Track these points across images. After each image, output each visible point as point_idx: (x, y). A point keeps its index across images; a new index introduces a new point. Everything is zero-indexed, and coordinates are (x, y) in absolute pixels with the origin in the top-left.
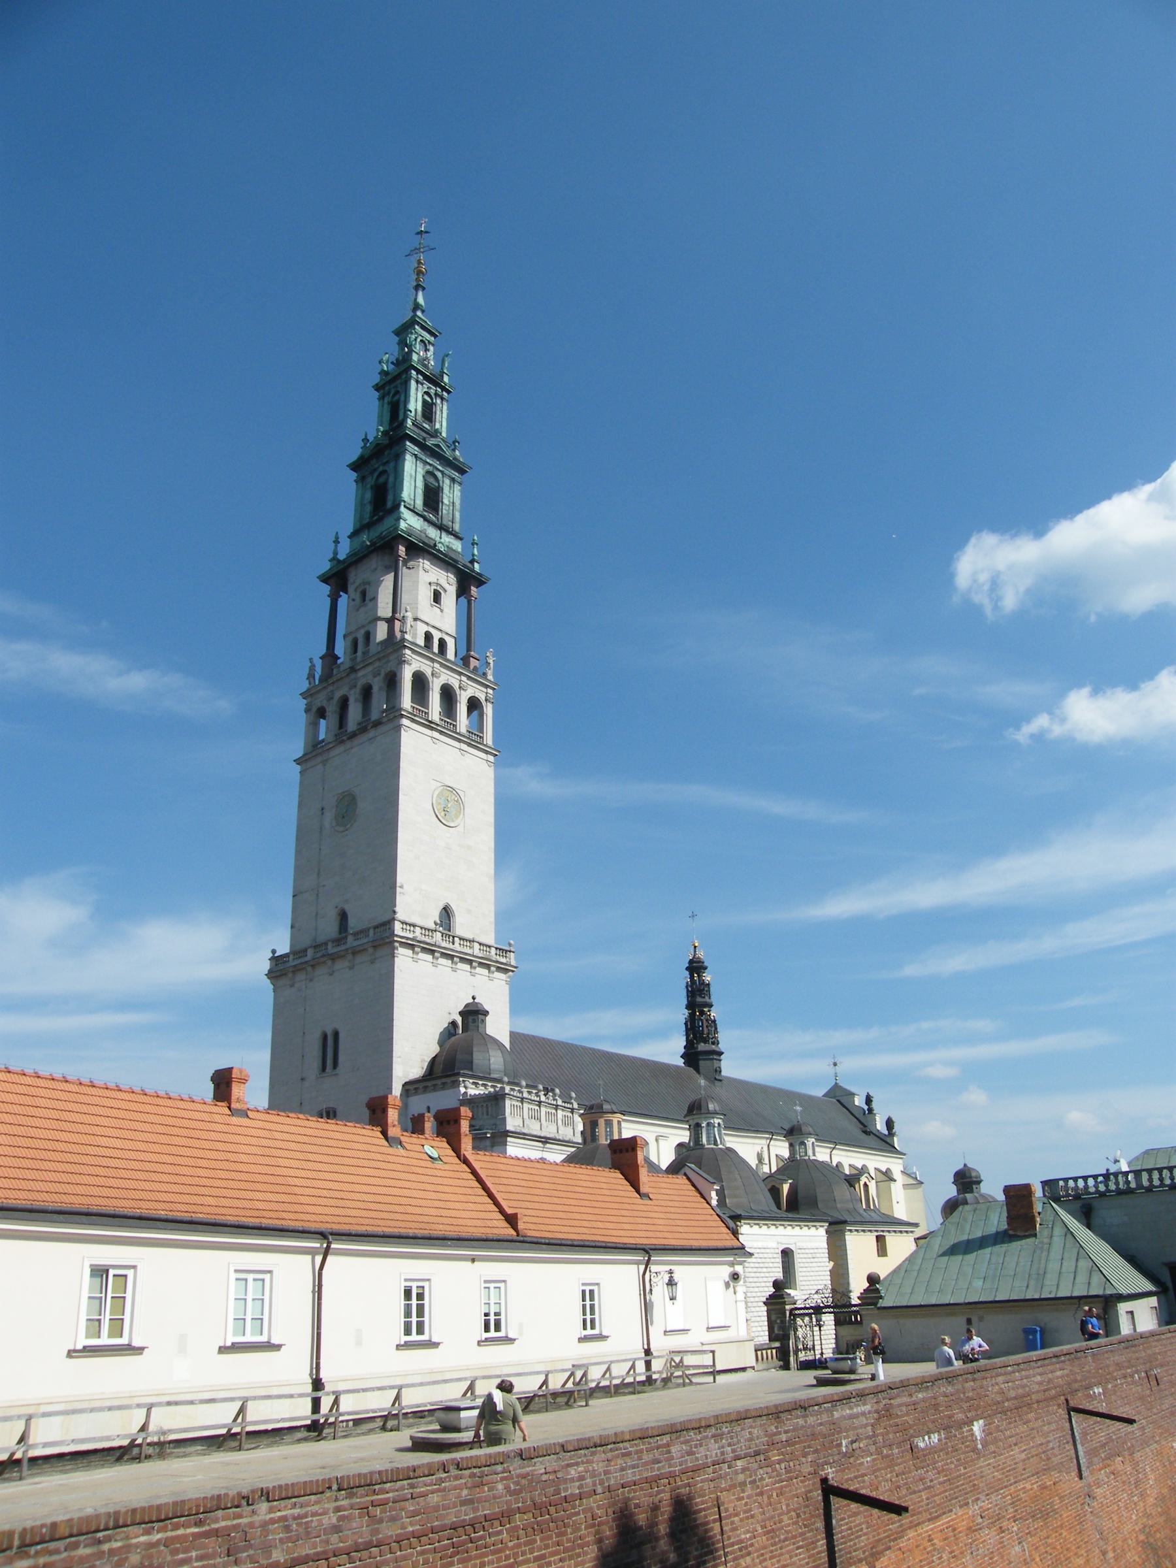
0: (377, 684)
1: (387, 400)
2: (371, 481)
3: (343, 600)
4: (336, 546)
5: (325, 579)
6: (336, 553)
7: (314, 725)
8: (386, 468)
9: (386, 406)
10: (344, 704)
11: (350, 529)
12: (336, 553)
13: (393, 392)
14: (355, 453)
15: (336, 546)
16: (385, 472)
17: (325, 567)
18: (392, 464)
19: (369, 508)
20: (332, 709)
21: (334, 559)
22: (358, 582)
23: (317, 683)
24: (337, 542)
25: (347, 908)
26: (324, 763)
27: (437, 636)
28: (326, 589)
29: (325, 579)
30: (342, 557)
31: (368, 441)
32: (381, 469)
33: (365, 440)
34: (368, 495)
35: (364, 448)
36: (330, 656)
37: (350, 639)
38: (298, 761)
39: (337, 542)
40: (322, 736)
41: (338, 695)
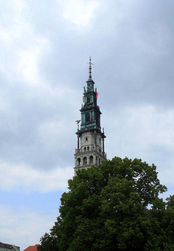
6: (78, 128)
12: (78, 128)
13: (88, 96)
14: (80, 108)
17: (77, 131)
22: (85, 136)
28: (77, 136)
33: (82, 105)
34: (84, 118)
36: (78, 149)
37: (84, 147)
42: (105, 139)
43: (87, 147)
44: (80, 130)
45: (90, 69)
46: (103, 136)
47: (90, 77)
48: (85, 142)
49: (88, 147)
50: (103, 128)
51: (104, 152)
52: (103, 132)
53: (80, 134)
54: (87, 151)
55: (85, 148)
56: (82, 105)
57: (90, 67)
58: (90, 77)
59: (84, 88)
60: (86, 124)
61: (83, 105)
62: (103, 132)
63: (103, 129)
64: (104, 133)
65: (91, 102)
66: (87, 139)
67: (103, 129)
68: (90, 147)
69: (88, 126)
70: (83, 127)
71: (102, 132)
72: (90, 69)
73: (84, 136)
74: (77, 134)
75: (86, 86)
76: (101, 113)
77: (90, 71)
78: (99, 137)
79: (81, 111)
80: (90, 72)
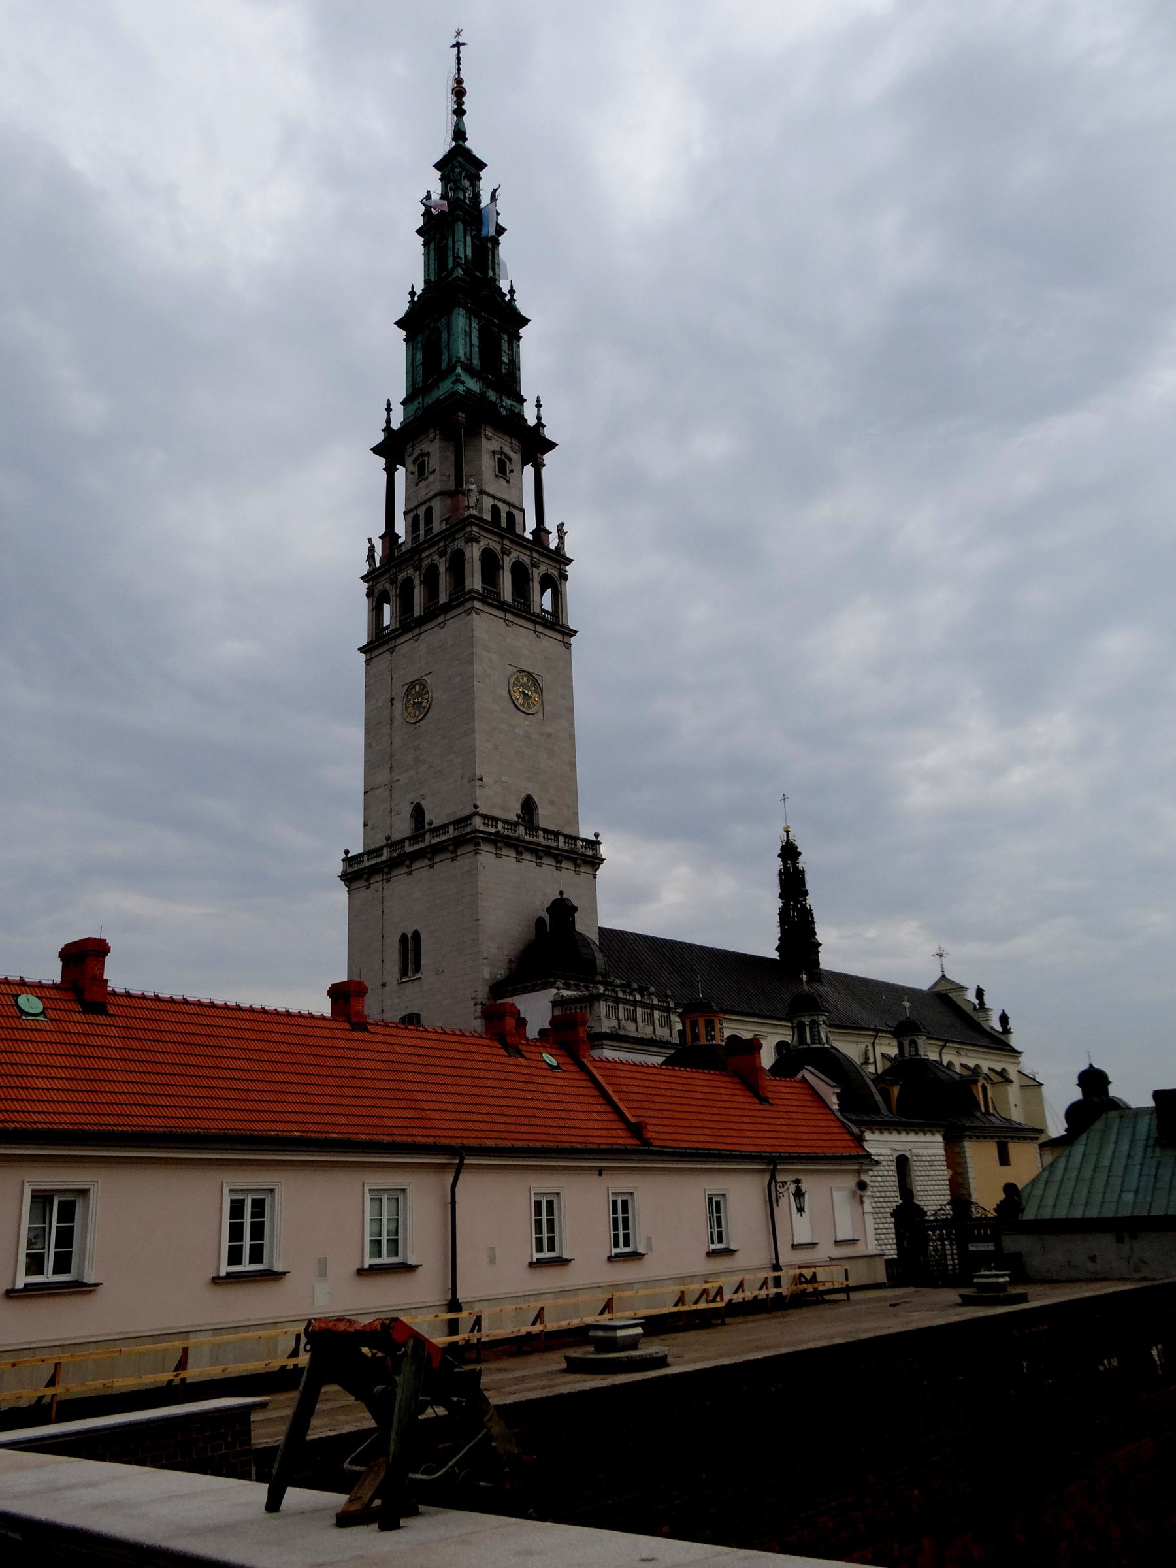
3: (400, 474)
4: (389, 414)
5: (377, 450)
6: (388, 421)
7: (376, 612)
9: (432, 253)
10: (408, 585)
11: (403, 395)
12: (388, 421)
15: (389, 414)
17: (379, 437)
19: (420, 371)
20: (393, 593)
21: (388, 429)
22: (417, 452)
23: (378, 565)
24: (389, 409)
25: (423, 803)
26: (391, 651)
27: (504, 509)
28: (381, 462)
29: (377, 450)
30: (396, 425)
31: (415, 294)
33: (412, 293)
34: (419, 356)
36: (389, 536)
37: (411, 515)
38: (362, 650)
39: (389, 409)
40: (387, 621)
43: (421, 511)
47: (459, 134)
50: (538, 401)
51: (541, 531)
52: (539, 418)
58: (459, 134)
62: (539, 418)
63: (539, 406)
64: (540, 425)
67: (539, 406)
68: (437, 505)
71: (532, 422)
75: (436, 189)
76: (525, 321)
80: (459, 112)
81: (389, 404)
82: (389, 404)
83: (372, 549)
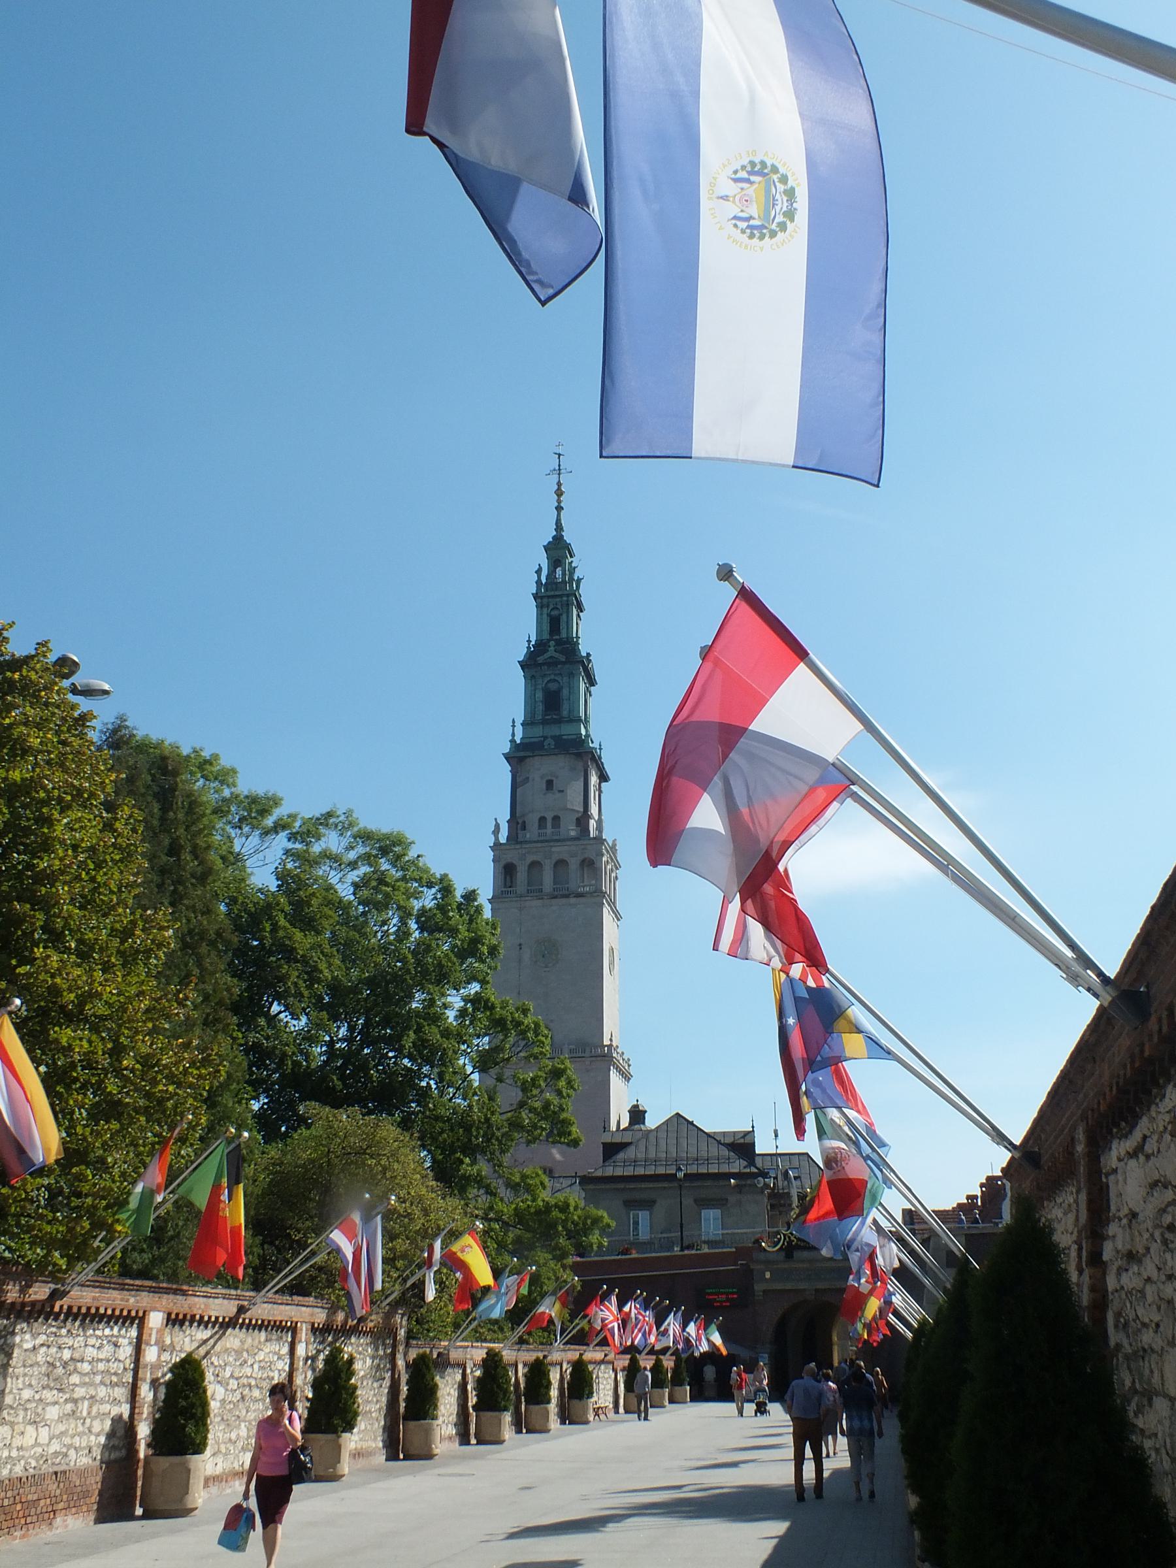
0: (574, 864)
1: (545, 611)
2: (541, 683)
6: (513, 735)
8: (559, 678)
9: (545, 616)
11: (520, 719)
12: (513, 735)
13: (551, 606)
14: (521, 654)
16: (555, 681)
17: (507, 748)
18: (565, 679)
19: (540, 707)
21: (513, 741)
24: (514, 726)
30: (518, 742)
32: (552, 677)
33: (529, 641)
34: (539, 695)
35: (529, 648)
39: (514, 726)
41: (530, 858)
42: (603, 784)
43: (549, 816)
44: (518, 742)
45: (559, 493)
46: (603, 777)
47: (559, 527)
48: (545, 794)
49: (556, 819)
53: (519, 756)
54: (549, 830)
55: (542, 820)
56: (529, 641)
57: (559, 484)
58: (559, 527)
59: (539, 572)
60: (544, 722)
61: (533, 643)
65: (564, 635)
66: (550, 784)
69: (554, 730)
70: (538, 731)
72: (559, 493)
73: (541, 768)
74: (508, 757)
77: (559, 501)
78: (594, 779)
79: (524, 665)
80: (559, 509)
81: (514, 721)
82: (514, 721)
83: (497, 827)
